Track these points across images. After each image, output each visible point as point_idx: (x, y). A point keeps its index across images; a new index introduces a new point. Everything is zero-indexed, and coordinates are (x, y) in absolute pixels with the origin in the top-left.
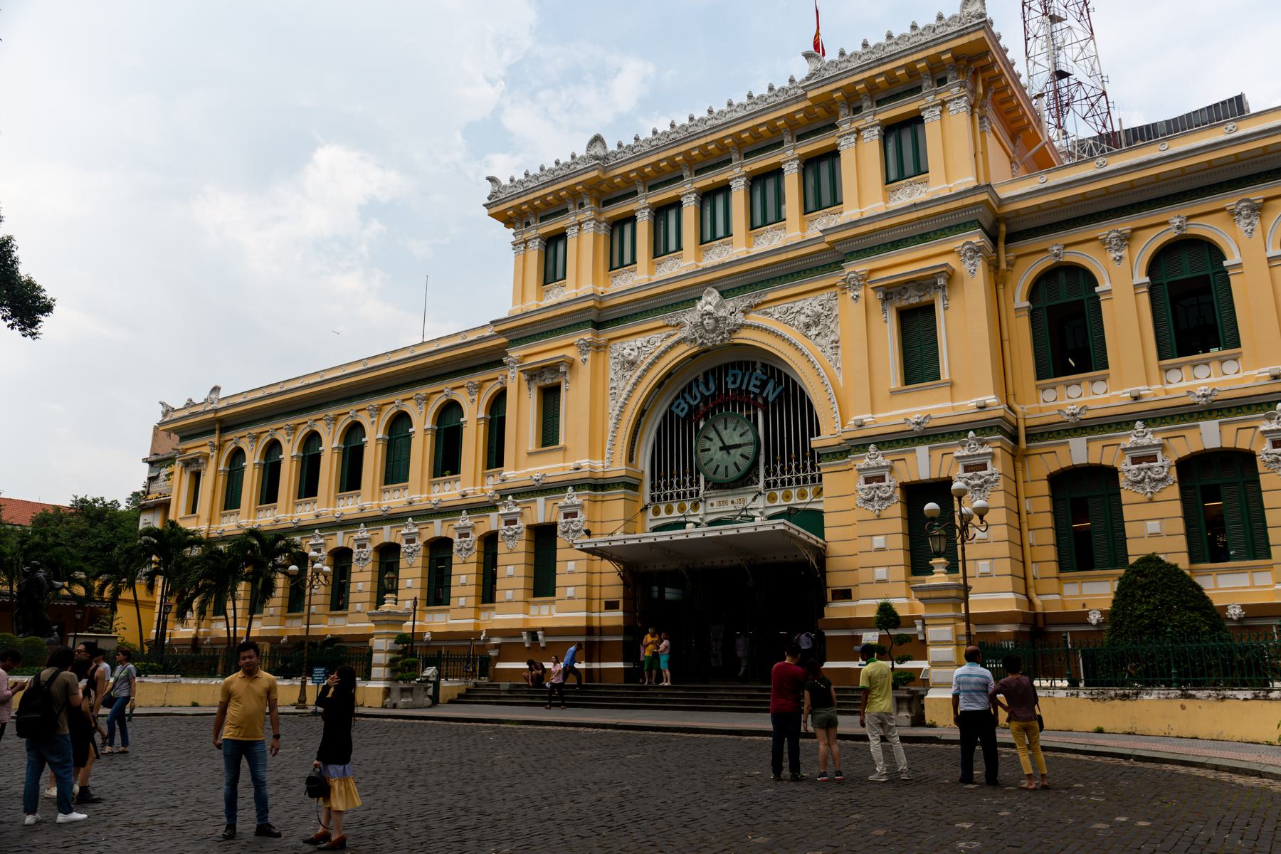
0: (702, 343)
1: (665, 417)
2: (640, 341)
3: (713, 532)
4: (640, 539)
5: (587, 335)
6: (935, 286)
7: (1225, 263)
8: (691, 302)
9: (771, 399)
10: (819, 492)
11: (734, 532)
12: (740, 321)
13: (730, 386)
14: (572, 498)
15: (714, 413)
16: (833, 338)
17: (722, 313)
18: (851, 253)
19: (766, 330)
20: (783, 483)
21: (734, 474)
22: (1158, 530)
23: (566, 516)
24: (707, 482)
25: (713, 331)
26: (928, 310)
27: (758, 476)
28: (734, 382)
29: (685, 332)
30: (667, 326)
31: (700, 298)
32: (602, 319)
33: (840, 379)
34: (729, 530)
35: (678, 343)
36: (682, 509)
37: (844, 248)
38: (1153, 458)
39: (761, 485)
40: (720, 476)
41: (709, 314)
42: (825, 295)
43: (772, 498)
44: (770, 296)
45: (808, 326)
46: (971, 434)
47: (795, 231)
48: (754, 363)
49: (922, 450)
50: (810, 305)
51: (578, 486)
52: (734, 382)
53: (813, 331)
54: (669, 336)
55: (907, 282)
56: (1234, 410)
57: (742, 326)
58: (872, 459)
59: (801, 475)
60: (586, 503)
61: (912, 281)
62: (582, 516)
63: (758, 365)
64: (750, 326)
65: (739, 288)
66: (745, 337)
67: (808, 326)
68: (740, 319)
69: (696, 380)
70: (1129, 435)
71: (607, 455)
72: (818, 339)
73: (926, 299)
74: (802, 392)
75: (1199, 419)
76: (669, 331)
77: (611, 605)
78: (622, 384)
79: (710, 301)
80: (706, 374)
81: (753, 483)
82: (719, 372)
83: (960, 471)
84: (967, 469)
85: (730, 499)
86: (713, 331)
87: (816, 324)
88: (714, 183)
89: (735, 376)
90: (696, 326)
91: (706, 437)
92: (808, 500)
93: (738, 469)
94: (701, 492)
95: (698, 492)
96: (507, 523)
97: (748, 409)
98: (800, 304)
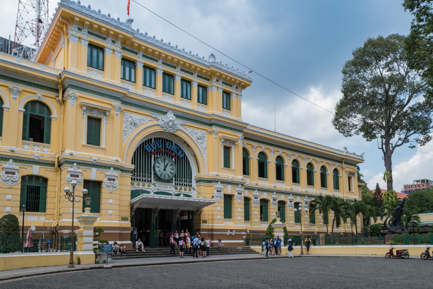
3: (157, 196)
6: (105, 114)
7: (3, 106)
8: (165, 113)
9: (181, 156)
10: (190, 190)
11: (171, 198)
12: (180, 128)
13: (167, 147)
14: (111, 172)
15: (157, 154)
16: (205, 146)
17: (175, 122)
19: (151, 126)
20: (148, 181)
21: (167, 178)
22: (11, 199)
24: (154, 178)
25: (170, 127)
26: (99, 120)
27: (172, 180)
28: (169, 146)
29: (160, 122)
30: (151, 116)
32: (127, 101)
33: (206, 159)
34: (163, 197)
35: (156, 125)
37: (213, 121)
38: (14, 173)
39: (174, 184)
40: (162, 177)
41: (173, 121)
42: (204, 132)
43: (176, 188)
44: (188, 124)
45: (198, 139)
46: (240, 185)
47: (192, 106)
48: (172, 142)
49: (230, 186)
50: (200, 133)
51: (116, 168)
52: (169, 146)
53: (200, 141)
54: (151, 121)
55: (229, 140)
56: (31, 162)
57: (180, 130)
58: (219, 185)
59: (139, 178)
60: (119, 176)
61: (230, 140)
63: (174, 144)
64: (182, 131)
65: (181, 116)
66: (179, 134)
67: (198, 139)
69: (151, 139)
70: (6, 163)
71: (125, 158)
72: (201, 144)
73: (230, 146)
74: (187, 157)
75: (34, 164)
76: (153, 120)
78: (130, 130)
79: (170, 116)
80: (155, 138)
81: (170, 182)
82: (164, 141)
83: (237, 194)
84: (238, 193)
85: (162, 186)
86: (170, 127)
87: (201, 139)
89: (169, 144)
90: (165, 122)
92: (146, 187)
94: (153, 181)
95: (151, 181)
96: (238, 193)
97: (169, 156)
98: (196, 131)
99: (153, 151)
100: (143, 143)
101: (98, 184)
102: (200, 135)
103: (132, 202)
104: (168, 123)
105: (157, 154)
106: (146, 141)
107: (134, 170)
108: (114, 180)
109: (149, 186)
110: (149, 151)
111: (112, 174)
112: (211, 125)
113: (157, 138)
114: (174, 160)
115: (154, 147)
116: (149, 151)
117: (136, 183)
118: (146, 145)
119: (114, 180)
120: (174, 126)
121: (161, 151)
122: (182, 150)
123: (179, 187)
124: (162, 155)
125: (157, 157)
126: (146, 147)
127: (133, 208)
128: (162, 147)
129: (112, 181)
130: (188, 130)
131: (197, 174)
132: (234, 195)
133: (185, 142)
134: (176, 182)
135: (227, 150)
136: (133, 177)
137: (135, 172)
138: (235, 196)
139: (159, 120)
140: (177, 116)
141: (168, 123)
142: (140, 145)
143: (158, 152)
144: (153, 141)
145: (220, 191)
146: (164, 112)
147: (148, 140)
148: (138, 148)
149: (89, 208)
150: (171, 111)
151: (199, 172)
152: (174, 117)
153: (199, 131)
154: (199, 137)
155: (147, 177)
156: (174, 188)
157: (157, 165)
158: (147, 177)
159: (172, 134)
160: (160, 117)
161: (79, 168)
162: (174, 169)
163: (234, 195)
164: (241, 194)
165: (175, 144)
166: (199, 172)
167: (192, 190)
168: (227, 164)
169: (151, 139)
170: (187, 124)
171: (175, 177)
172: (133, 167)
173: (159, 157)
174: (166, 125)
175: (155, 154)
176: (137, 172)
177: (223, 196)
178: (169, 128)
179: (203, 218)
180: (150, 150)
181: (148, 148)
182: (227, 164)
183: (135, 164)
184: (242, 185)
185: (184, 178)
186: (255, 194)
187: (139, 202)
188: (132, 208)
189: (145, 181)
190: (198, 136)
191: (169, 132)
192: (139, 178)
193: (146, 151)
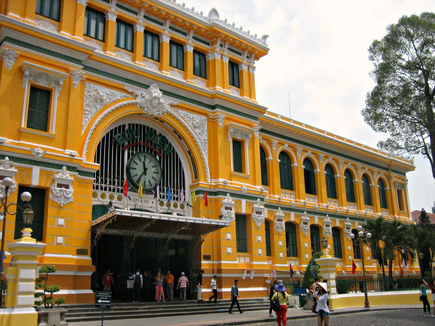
0: (146, 111)
1: (103, 139)
2: (107, 90)
4: (203, 221)
5: (77, 69)
8: (147, 87)
12: (169, 110)
14: (65, 175)
15: (133, 149)
17: (162, 101)
18: (219, 105)
23: (59, 186)
31: (149, 86)
36: (111, 197)
37: (217, 102)
42: (204, 117)
43: (162, 204)
45: (195, 127)
48: (155, 131)
49: (244, 201)
50: (198, 119)
53: (197, 131)
57: (168, 113)
58: (228, 200)
62: (71, 189)
63: (158, 133)
64: (171, 115)
67: (195, 127)
68: (169, 109)
69: (124, 126)
76: (128, 95)
77: (80, 252)
78: (94, 110)
80: (129, 125)
87: (199, 128)
88: (153, 30)
89: (151, 134)
90: (146, 100)
91: (156, 166)
93: (151, 185)
98: (191, 115)
99: (127, 143)
100: (112, 131)
101: (40, 194)
102: (197, 121)
103: (95, 224)
104: (151, 101)
105: (133, 149)
106: (116, 129)
107: (98, 172)
108: (67, 187)
109: (120, 199)
110: (121, 143)
111: (64, 177)
112: (213, 107)
113: (133, 125)
114: (158, 158)
115: (129, 136)
116: (121, 143)
117: (99, 192)
118: (115, 134)
119: (67, 187)
120: (160, 106)
121: (137, 146)
122: (170, 145)
123: (165, 201)
124: (140, 150)
125: (132, 154)
126: (116, 137)
127: (96, 234)
128: (140, 139)
129: (63, 189)
130: (180, 114)
131: (193, 182)
132: (250, 215)
133: (176, 132)
134: (162, 194)
135: (238, 145)
136: (95, 184)
137: (98, 175)
138: (253, 216)
139: (137, 96)
140: (165, 93)
141: (151, 101)
142: (107, 135)
143: (133, 145)
144: (127, 128)
145: (231, 209)
146: (145, 85)
147: (120, 127)
148: (104, 137)
149: (30, 230)
150: (155, 84)
151: (196, 177)
152: (161, 94)
153: (196, 116)
154: (197, 125)
155: (116, 184)
156: (159, 203)
157: (133, 165)
158: (116, 184)
159: (156, 118)
160: (139, 91)
161: (11, 166)
162: (158, 173)
163: (250, 215)
164: (260, 213)
165: (160, 135)
166: (196, 177)
167: (186, 206)
168: (239, 166)
169: (124, 126)
170: (178, 104)
171: (160, 185)
172: (97, 166)
173: (136, 154)
174: (148, 104)
175: (129, 149)
176: (102, 176)
177: (233, 216)
178: (151, 109)
179: (205, 249)
180: (122, 142)
181: (120, 138)
182: (239, 166)
183: (98, 162)
184: (262, 199)
185: (174, 187)
186: (278, 214)
187: (107, 224)
188: (93, 234)
189: (114, 190)
190: (194, 122)
191: (152, 115)
192: (104, 185)
193: (116, 142)
